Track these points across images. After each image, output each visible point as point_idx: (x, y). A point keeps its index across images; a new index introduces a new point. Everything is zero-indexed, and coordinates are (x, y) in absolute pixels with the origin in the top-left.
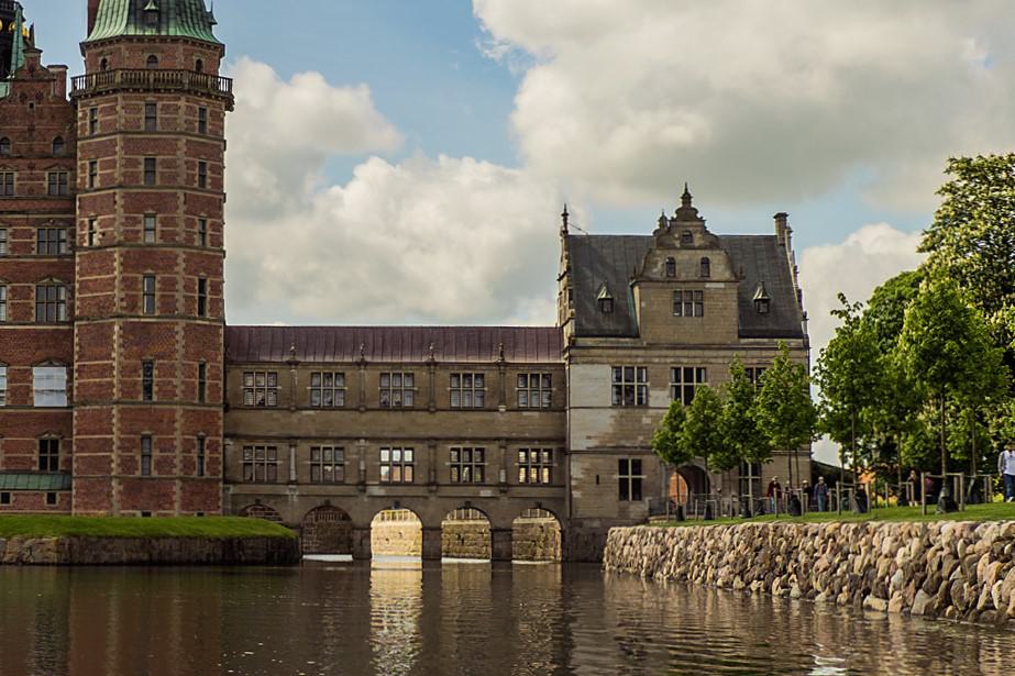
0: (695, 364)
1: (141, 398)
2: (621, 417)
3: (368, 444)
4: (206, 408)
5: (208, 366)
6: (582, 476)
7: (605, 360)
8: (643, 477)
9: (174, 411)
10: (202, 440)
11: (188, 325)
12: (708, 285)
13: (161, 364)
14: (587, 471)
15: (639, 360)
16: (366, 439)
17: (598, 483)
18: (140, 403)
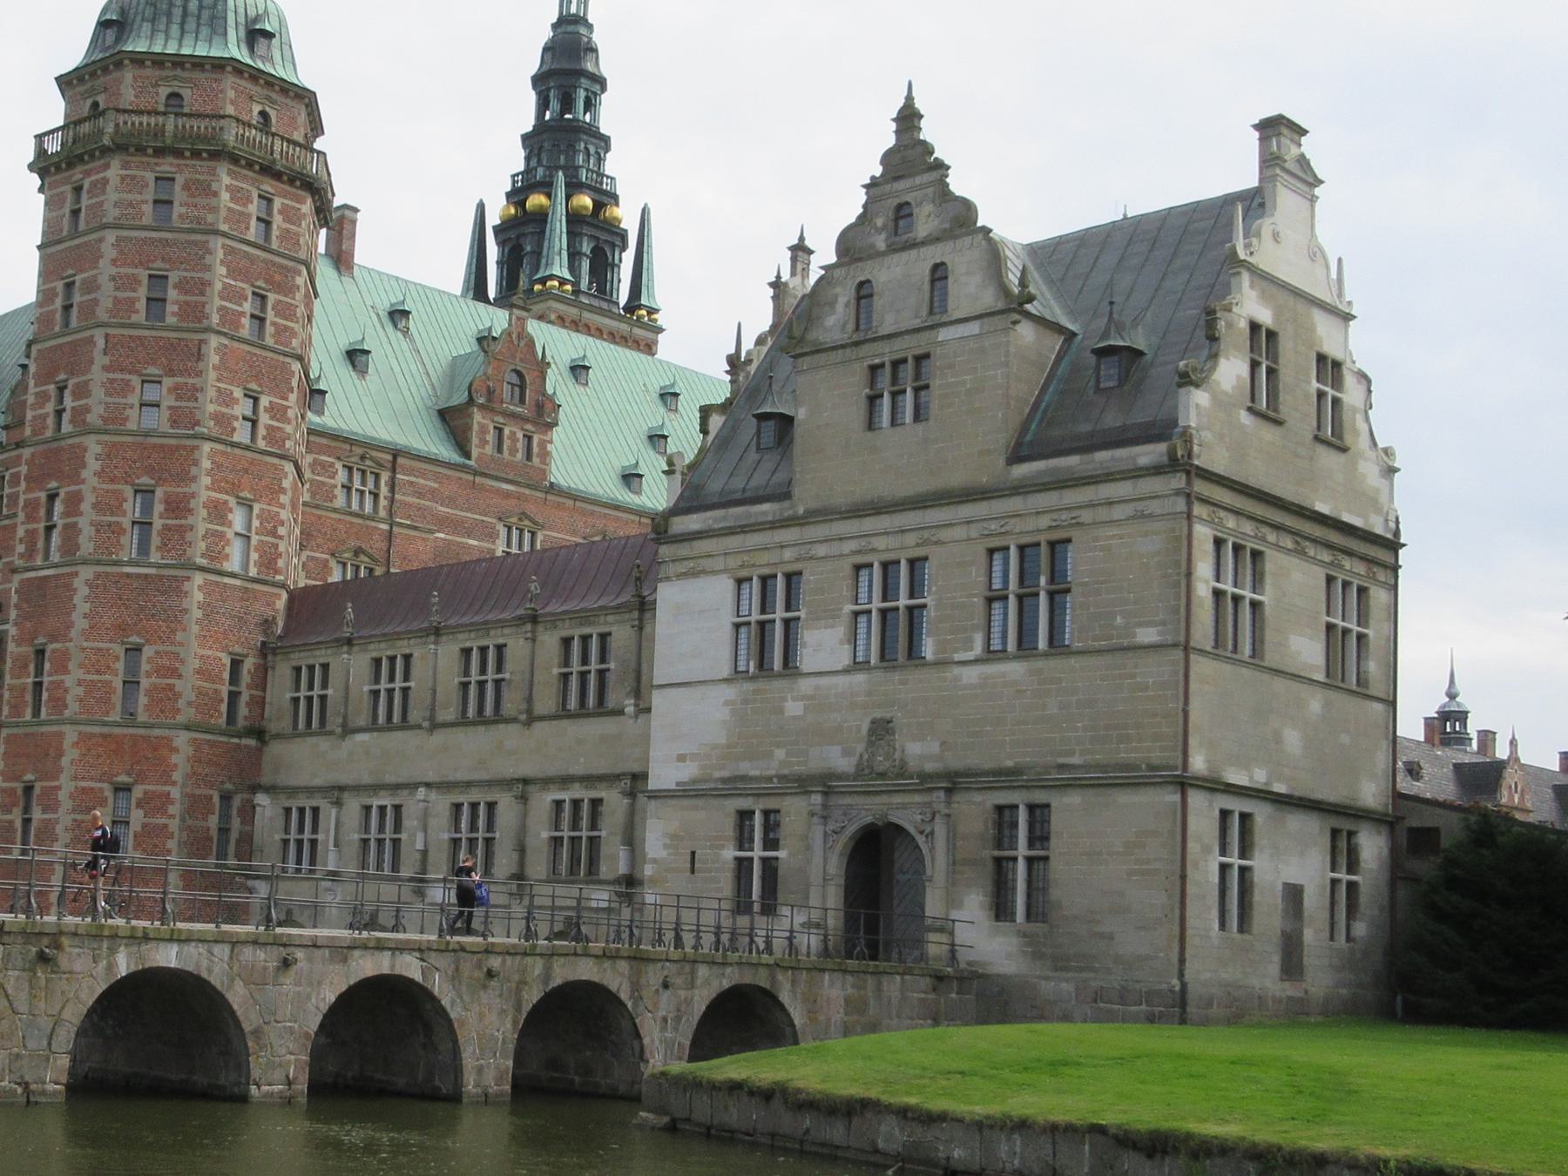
0: (903, 548)
1: (28, 716)
2: (745, 701)
3: (433, 796)
4: (141, 731)
5: (148, 651)
6: (663, 854)
7: (719, 563)
8: (781, 854)
9: (61, 735)
10: (122, 789)
11: (98, 576)
12: (944, 334)
13: (54, 651)
14: (675, 839)
15: (788, 554)
16: (428, 785)
17: (693, 871)
18: (27, 724)
